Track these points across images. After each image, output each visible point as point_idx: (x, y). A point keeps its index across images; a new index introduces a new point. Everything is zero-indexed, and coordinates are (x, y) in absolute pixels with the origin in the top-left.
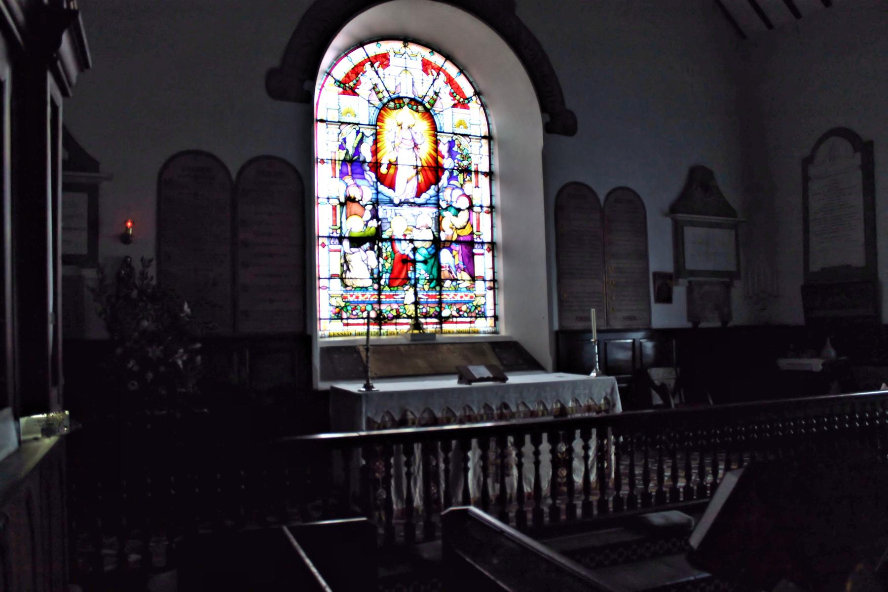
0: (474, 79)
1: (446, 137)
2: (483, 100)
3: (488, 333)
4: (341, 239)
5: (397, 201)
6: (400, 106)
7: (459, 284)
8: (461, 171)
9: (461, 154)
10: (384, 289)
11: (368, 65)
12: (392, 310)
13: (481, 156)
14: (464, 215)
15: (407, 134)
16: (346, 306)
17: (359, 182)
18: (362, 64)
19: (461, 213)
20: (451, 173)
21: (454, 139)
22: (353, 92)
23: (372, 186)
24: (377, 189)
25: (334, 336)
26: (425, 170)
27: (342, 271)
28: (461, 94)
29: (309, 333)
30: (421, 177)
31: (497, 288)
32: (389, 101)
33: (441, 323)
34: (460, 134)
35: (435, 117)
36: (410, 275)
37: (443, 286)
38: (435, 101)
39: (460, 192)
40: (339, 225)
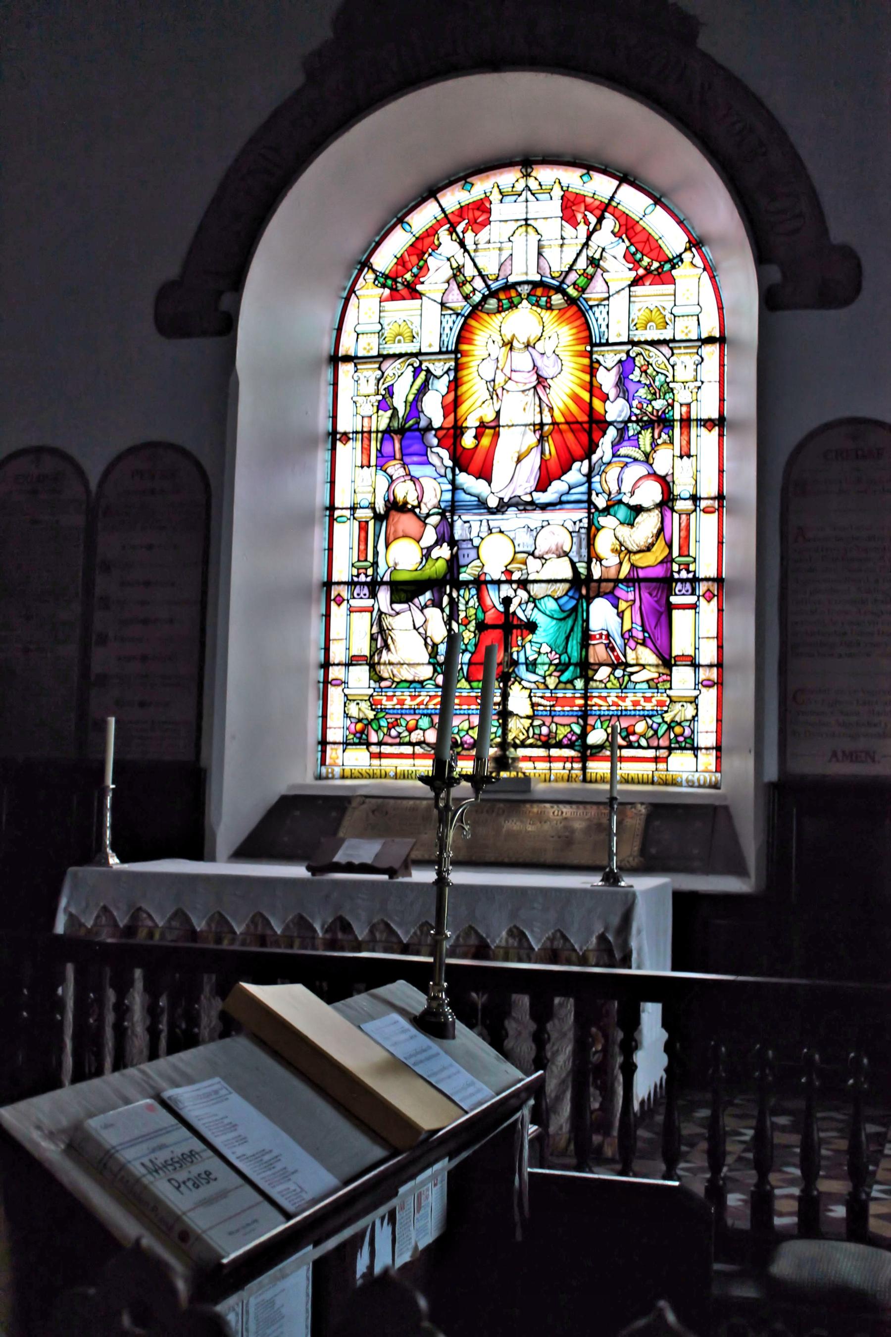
0: (685, 215)
1: (612, 354)
4: (373, 587)
5: (493, 503)
6: (511, 302)
7: (632, 673)
8: (649, 424)
11: (443, 233)
13: (699, 384)
14: (648, 523)
16: (376, 718)
17: (416, 470)
18: (432, 232)
20: (622, 431)
22: (413, 293)
23: (442, 476)
24: (453, 482)
25: (352, 777)
26: (561, 432)
27: (373, 649)
28: (654, 254)
29: (203, 763)
30: (550, 447)
32: (485, 299)
33: (584, 759)
35: (590, 316)
36: (515, 656)
37: (592, 679)
38: (591, 278)
39: (642, 470)
40: (370, 558)
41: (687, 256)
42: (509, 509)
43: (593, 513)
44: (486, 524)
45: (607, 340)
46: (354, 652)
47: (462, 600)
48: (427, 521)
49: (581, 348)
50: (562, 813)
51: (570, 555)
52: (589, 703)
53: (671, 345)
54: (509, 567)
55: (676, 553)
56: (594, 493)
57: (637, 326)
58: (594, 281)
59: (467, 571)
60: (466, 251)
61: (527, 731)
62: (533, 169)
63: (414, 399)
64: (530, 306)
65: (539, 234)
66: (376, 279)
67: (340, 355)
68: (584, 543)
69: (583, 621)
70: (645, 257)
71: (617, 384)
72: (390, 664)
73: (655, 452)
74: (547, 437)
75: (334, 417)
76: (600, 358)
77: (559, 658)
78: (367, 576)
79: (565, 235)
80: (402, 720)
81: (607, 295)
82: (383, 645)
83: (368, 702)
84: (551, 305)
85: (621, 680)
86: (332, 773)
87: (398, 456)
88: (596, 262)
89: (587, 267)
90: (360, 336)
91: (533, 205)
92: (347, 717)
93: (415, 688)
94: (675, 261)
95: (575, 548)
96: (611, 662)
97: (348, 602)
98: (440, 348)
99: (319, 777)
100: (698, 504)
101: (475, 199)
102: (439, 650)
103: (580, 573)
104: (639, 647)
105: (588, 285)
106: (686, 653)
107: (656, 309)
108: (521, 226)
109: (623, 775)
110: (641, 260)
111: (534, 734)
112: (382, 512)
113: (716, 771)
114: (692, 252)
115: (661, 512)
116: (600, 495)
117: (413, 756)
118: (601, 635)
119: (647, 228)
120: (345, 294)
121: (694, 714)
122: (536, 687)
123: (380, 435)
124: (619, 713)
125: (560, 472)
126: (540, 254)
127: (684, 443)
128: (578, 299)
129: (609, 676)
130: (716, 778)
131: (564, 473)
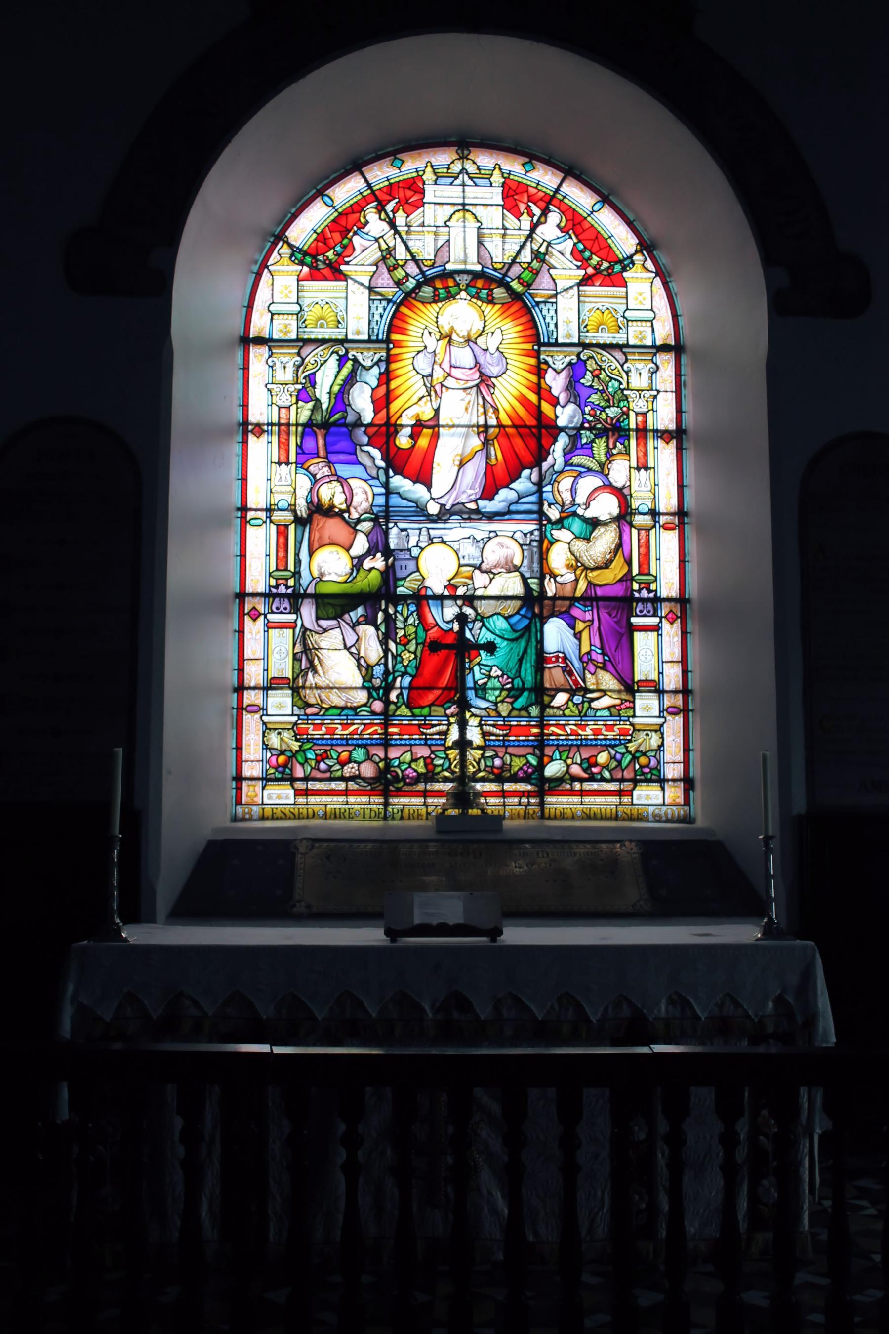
2: (663, 260)
3: (668, 821)
5: (433, 509)
7: (593, 700)
8: (602, 433)
9: (602, 392)
10: (398, 713)
12: (414, 760)
13: (655, 393)
14: (606, 539)
15: (463, 356)
16: (301, 750)
17: (343, 470)
18: (357, 208)
19: (601, 530)
20: (575, 438)
21: (583, 357)
22: (336, 273)
23: (373, 478)
24: (386, 485)
25: (273, 818)
26: (507, 435)
27: (297, 671)
28: (604, 253)
30: (496, 452)
31: (692, 710)
32: (419, 285)
34: (598, 346)
35: (536, 312)
37: (549, 706)
38: (536, 273)
40: (291, 567)
41: (638, 258)
42: (452, 518)
43: (545, 525)
44: (426, 533)
45: (556, 339)
46: (273, 673)
47: (399, 617)
48: (358, 527)
49: (529, 346)
50: (548, 854)
51: (522, 569)
52: (546, 731)
53: (624, 350)
54: (452, 582)
55: (635, 570)
56: (546, 504)
57: (589, 327)
58: (539, 276)
59: (405, 585)
60: (397, 232)
61: (478, 763)
62: (470, 152)
63: (340, 391)
64: (469, 298)
65: (478, 221)
66: (292, 255)
67: (251, 336)
68: (536, 557)
69: (537, 642)
70: (594, 256)
71: (567, 387)
72: (318, 687)
73: (610, 463)
74: (493, 440)
75: (245, 406)
76: (549, 359)
77: (512, 683)
78: (287, 587)
79: (507, 225)
80: (332, 751)
81: (554, 292)
82: (308, 666)
83: (291, 731)
84: (493, 298)
85: (580, 707)
86: (249, 813)
87: (322, 453)
88: (542, 257)
89: (532, 261)
90: (275, 317)
91: (471, 191)
92: (267, 749)
93: (347, 716)
94: (626, 263)
95: (526, 562)
96: (569, 687)
97: (265, 617)
98: (369, 336)
99: (235, 819)
100: (657, 520)
101: (406, 177)
102: (374, 673)
103: (532, 589)
104: (598, 670)
105: (534, 280)
106: (650, 678)
107: (607, 312)
108: (458, 211)
109: (584, 810)
110: (590, 258)
111: (486, 766)
112: (305, 515)
113: (685, 805)
114: (644, 255)
115: (619, 527)
116: (552, 506)
117: (346, 793)
118: (557, 657)
119: (596, 226)
120: (255, 268)
121: (660, 743)
123: (300, 429)
124: (579, 742)
125: (508, 479)
126: (480, 243)
127: (641, 454)
128: (524, 294)
129: (567, 703)
130: (685, 811)
131: (514, 481)
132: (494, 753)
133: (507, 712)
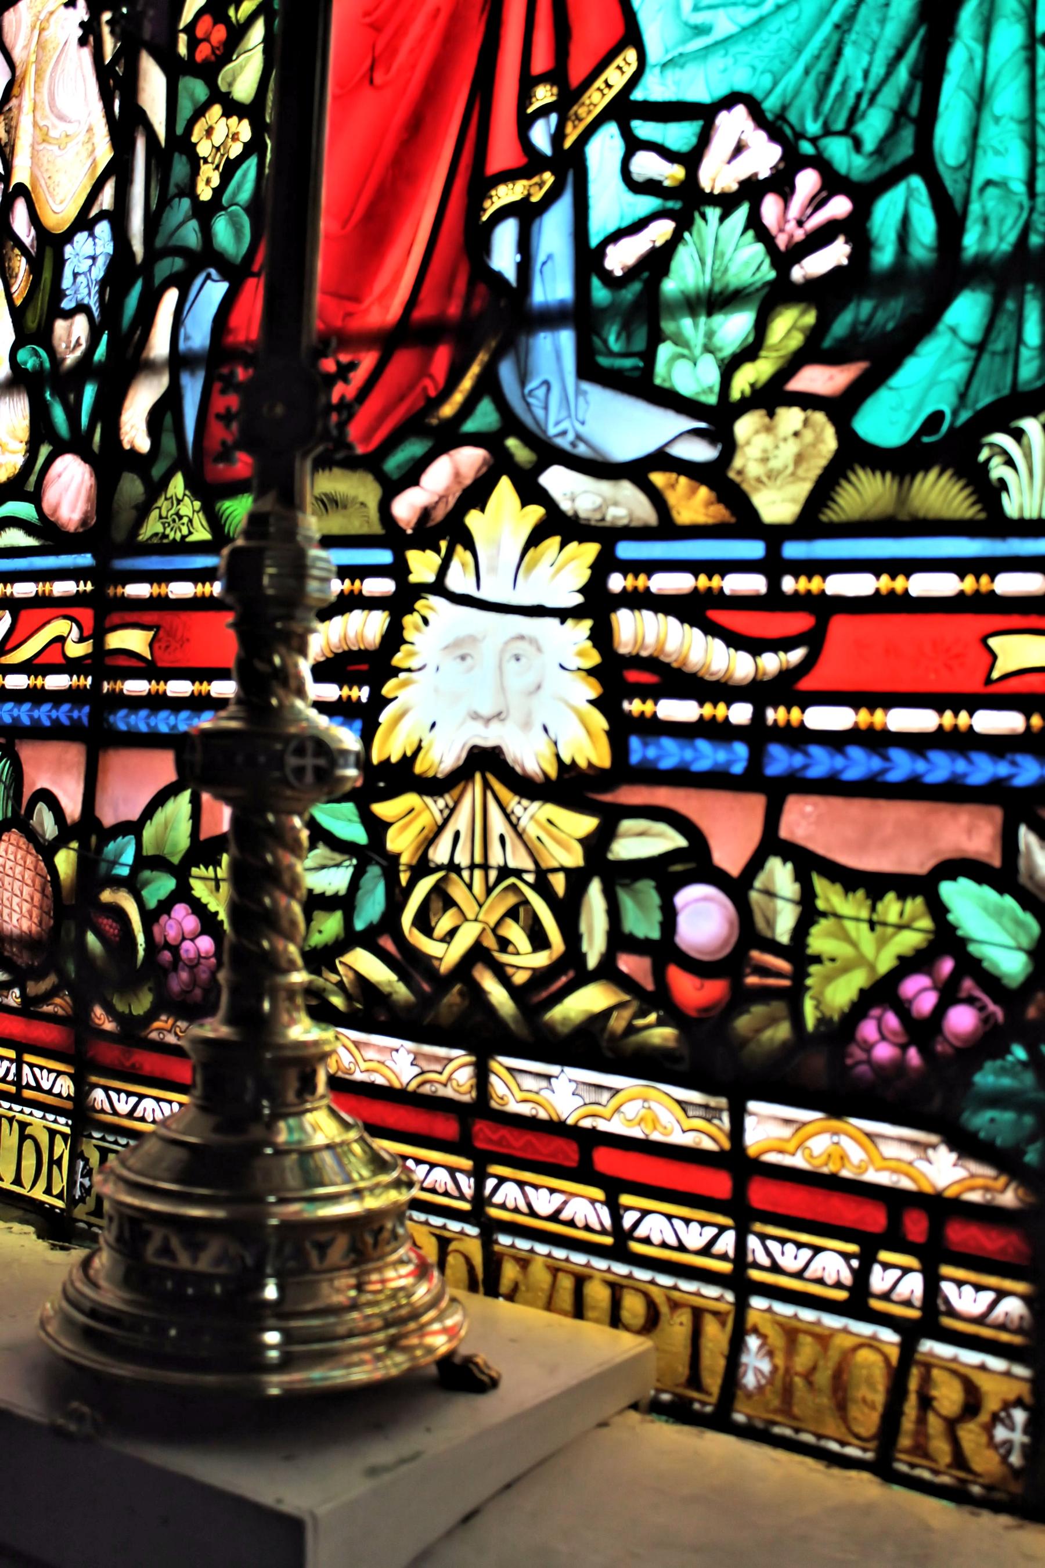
102: (67, 282)
122: (644, 511)
132: (678, 841)
133: (803, 489)
